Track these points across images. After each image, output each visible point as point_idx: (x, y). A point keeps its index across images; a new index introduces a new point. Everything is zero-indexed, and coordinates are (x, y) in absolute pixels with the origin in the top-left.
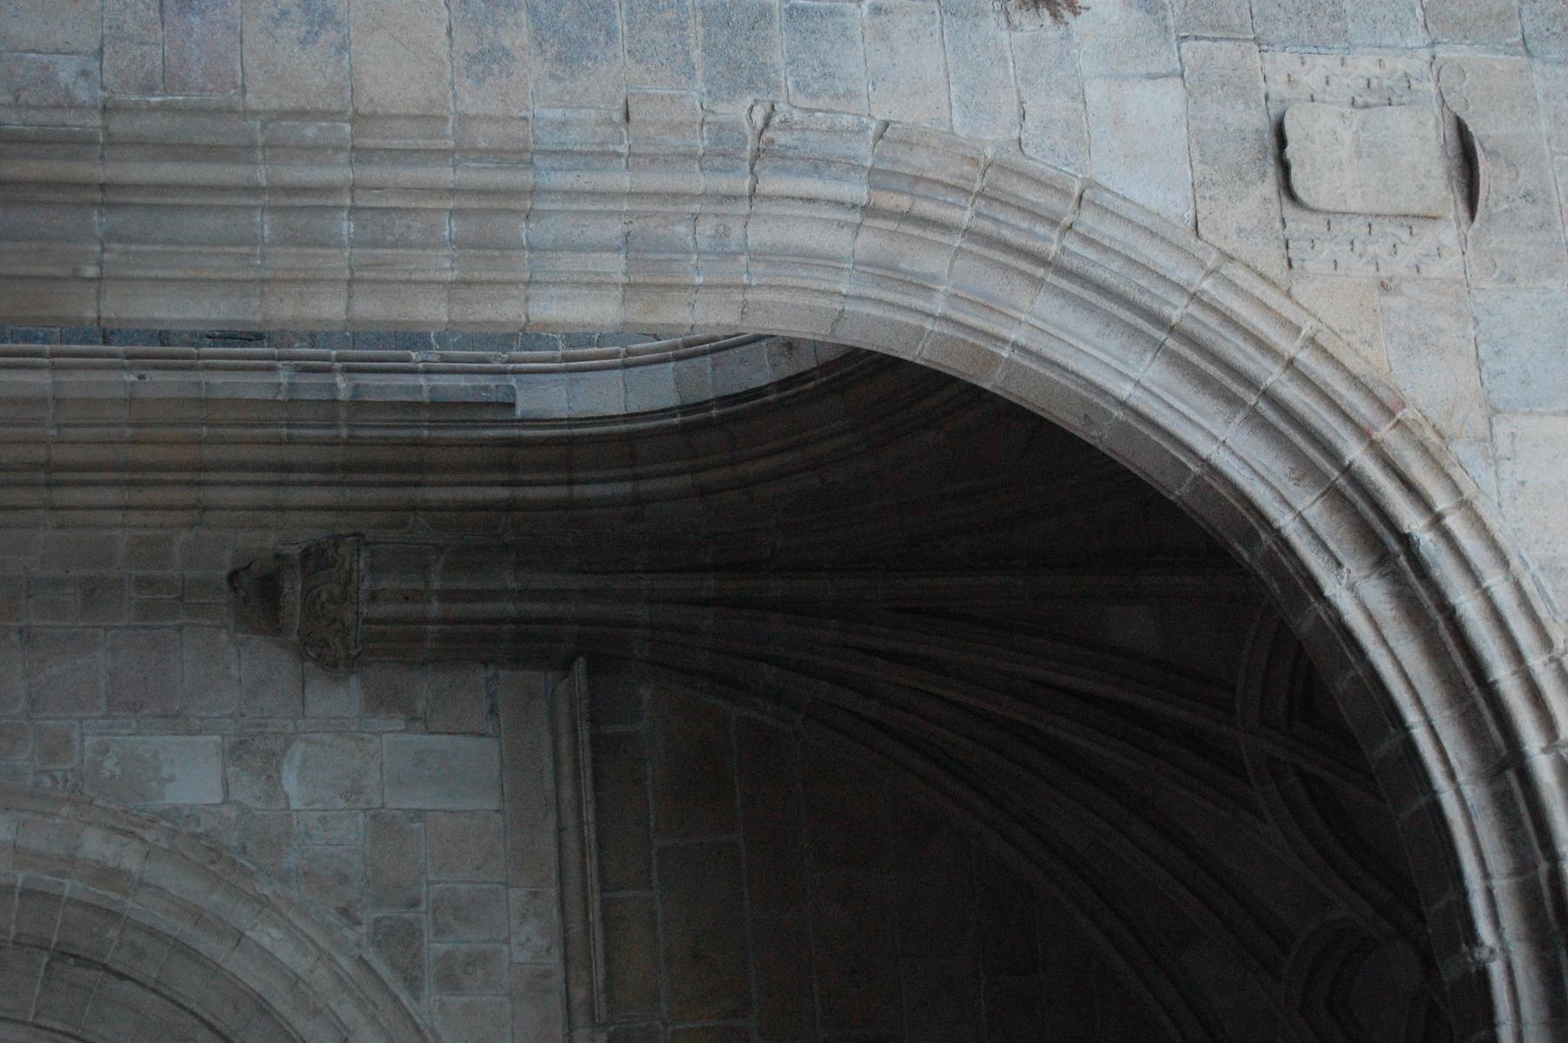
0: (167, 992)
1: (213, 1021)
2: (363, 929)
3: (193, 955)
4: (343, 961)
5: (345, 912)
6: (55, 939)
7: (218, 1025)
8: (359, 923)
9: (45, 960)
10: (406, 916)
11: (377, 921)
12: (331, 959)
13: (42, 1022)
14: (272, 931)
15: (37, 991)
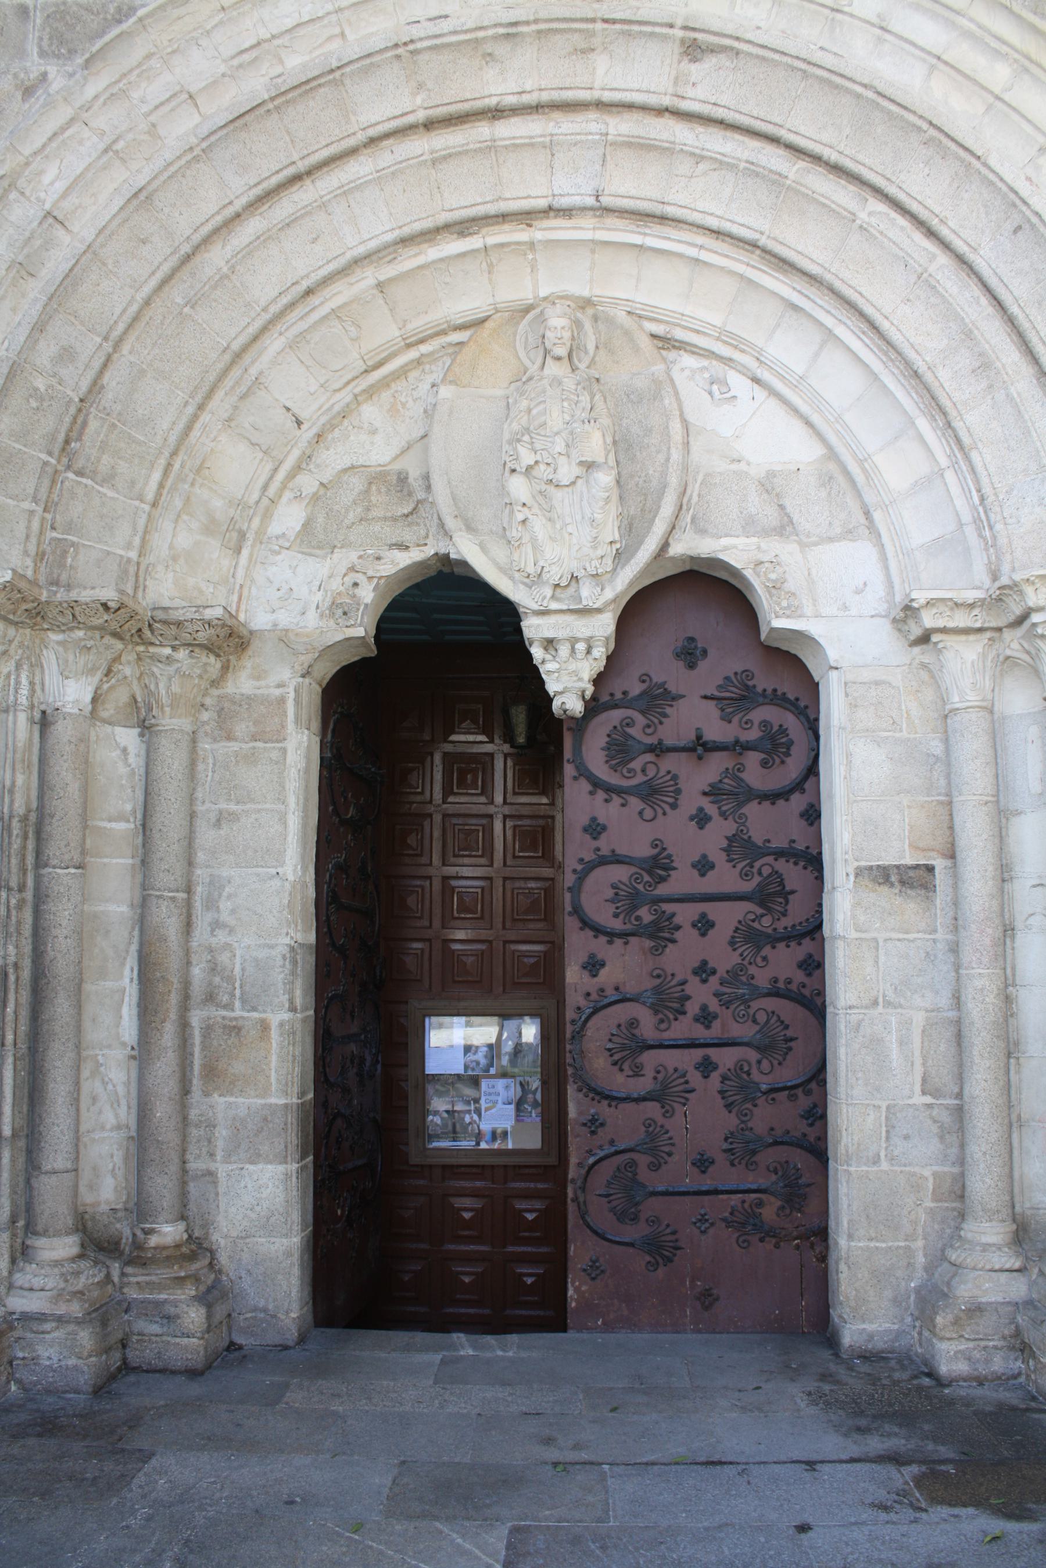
0: (121, 327)
1: (159, 276)
2: (52, 70)
3: (70, 280)
4: (90, 91)
5: (28, 92)
6: (44, 457)
7: (166, 268)
8: (44, 76)
9: (71, 475)
10: (38, 21)
11: (42, 54)
12: (87, 107)
13: (150, 496)
14: (47, 179)
15: (111, 494)
